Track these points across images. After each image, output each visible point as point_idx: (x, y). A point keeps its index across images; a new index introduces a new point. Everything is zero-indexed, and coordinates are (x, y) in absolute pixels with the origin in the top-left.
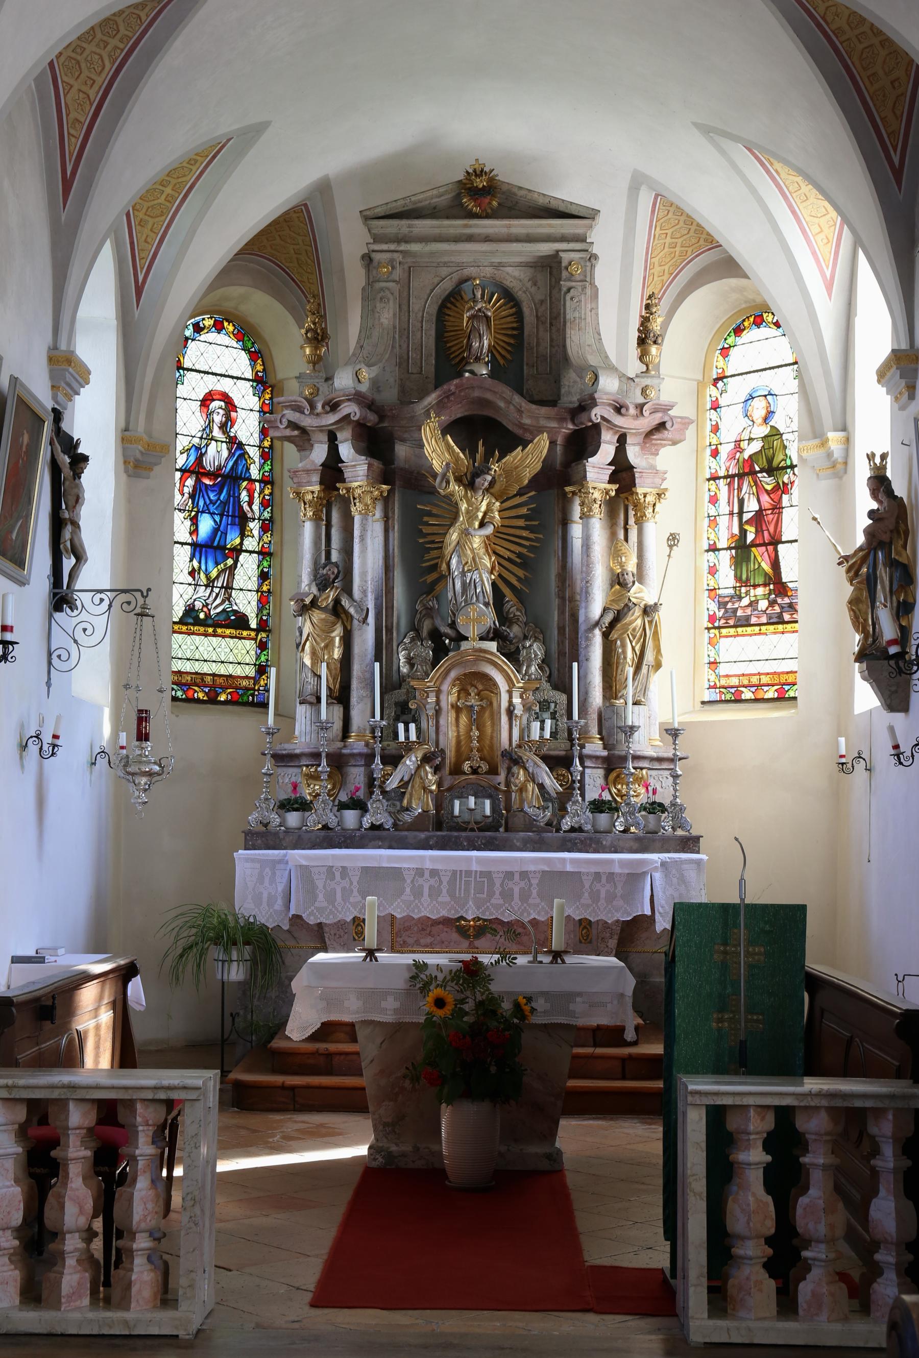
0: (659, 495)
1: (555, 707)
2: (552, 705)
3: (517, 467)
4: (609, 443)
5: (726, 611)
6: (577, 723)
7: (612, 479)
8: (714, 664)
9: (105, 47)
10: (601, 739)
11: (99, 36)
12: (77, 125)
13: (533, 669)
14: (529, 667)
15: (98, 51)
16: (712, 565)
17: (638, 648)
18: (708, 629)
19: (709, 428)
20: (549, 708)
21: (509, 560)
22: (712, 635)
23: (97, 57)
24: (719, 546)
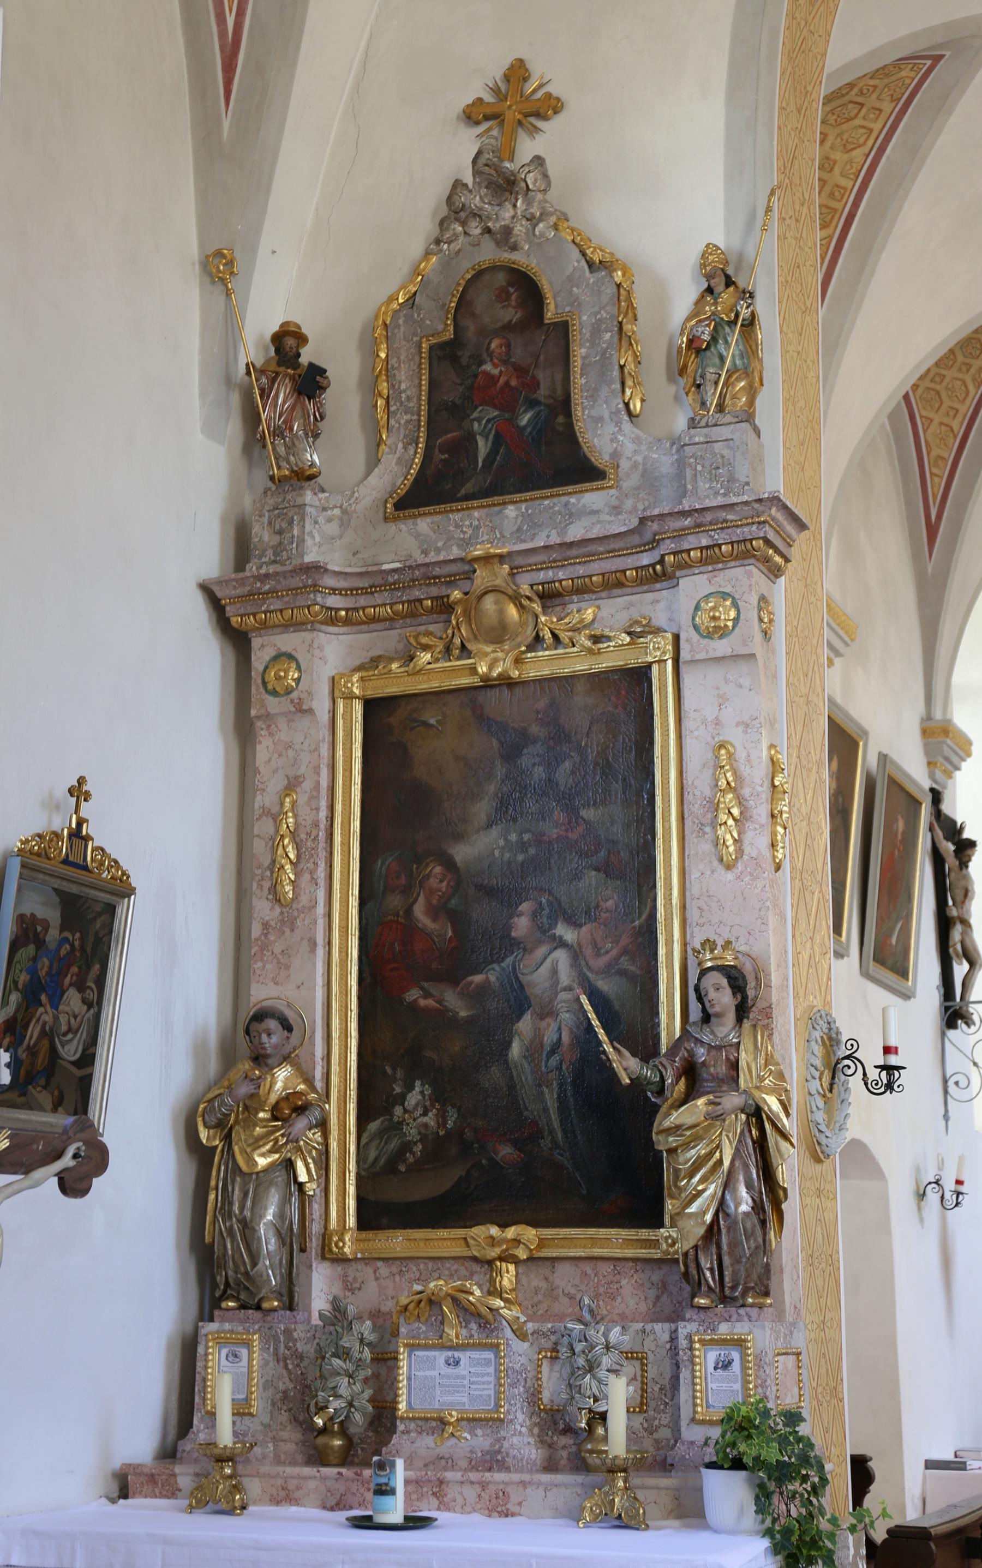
9: (968, 370)
11: (960, 358)
12: (940, 463)
15: (960, 376)
23: (959, 383)
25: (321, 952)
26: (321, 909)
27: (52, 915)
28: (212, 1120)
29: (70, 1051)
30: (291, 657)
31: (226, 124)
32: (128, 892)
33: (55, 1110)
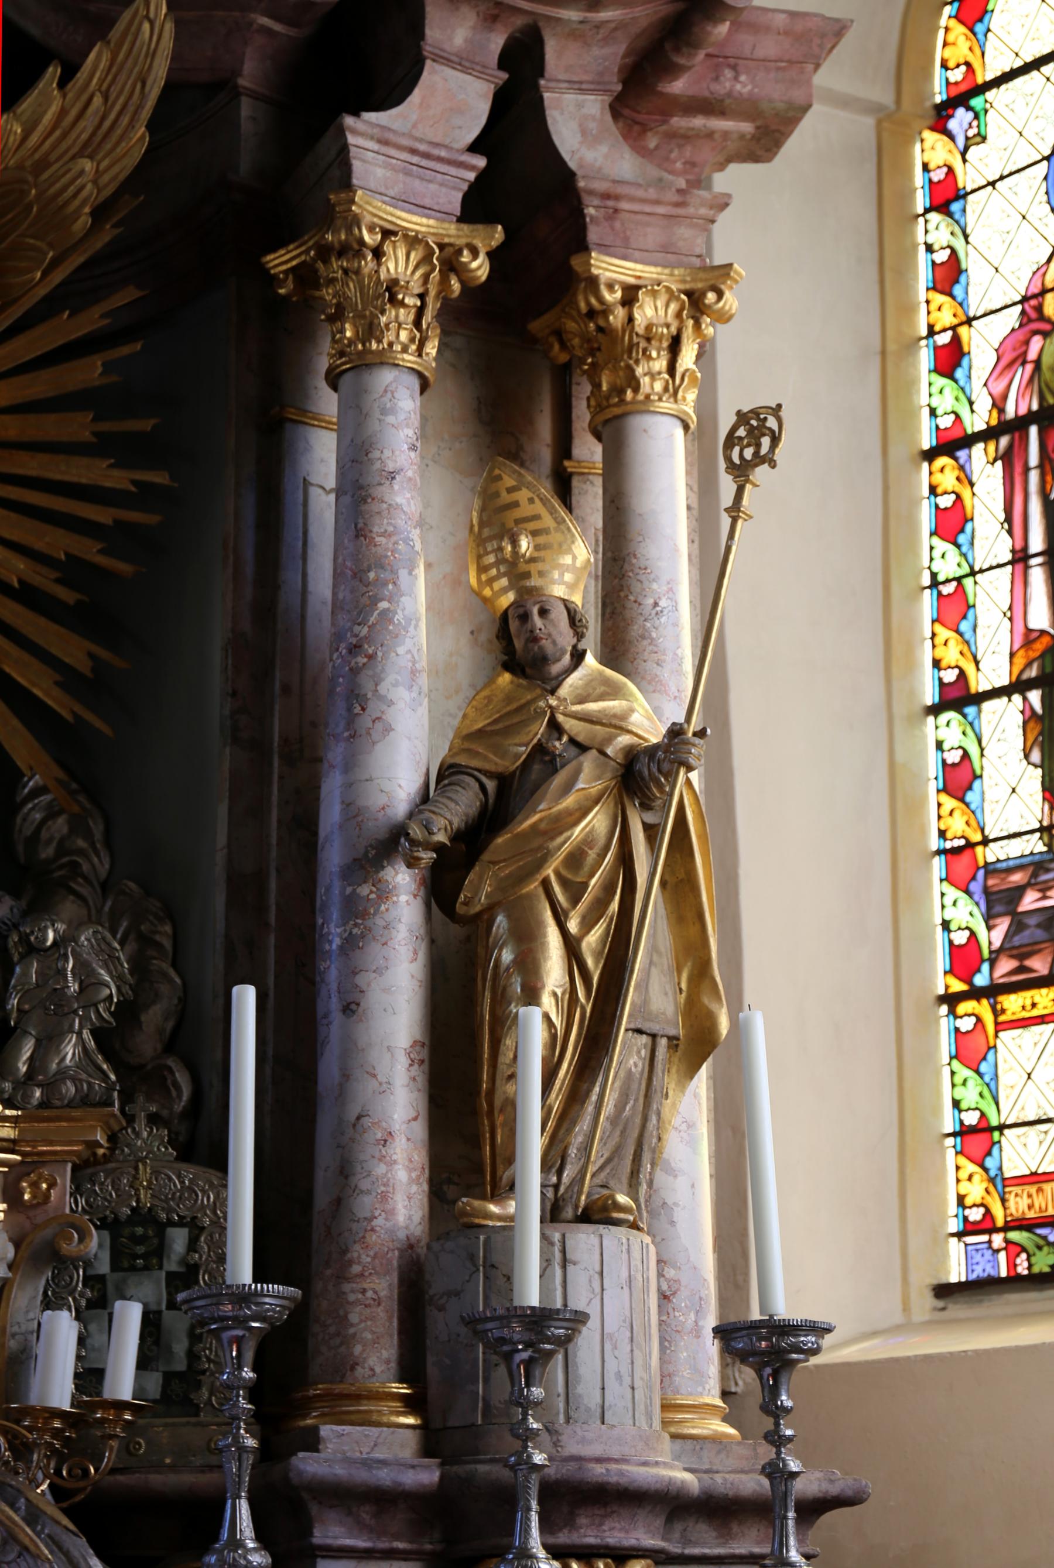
0: (695, 304)
1: (192, 1245)
2: (178, 1239)
3: (42, 165)
4: (462, 63)
5: (1018, 924)
6: (243, 1297)
7: (475, 207)
8: (978, 1137)
10: (411, 1404)
13: (70, 1051)
14: (48, 1042)
16: (954, 757)
17: (592, 940)
18: (951, 1000)
19: (924, 275)
20: (160, 1251)
21: (26, 595)
22: (966, 1024)
24: (979, 683)
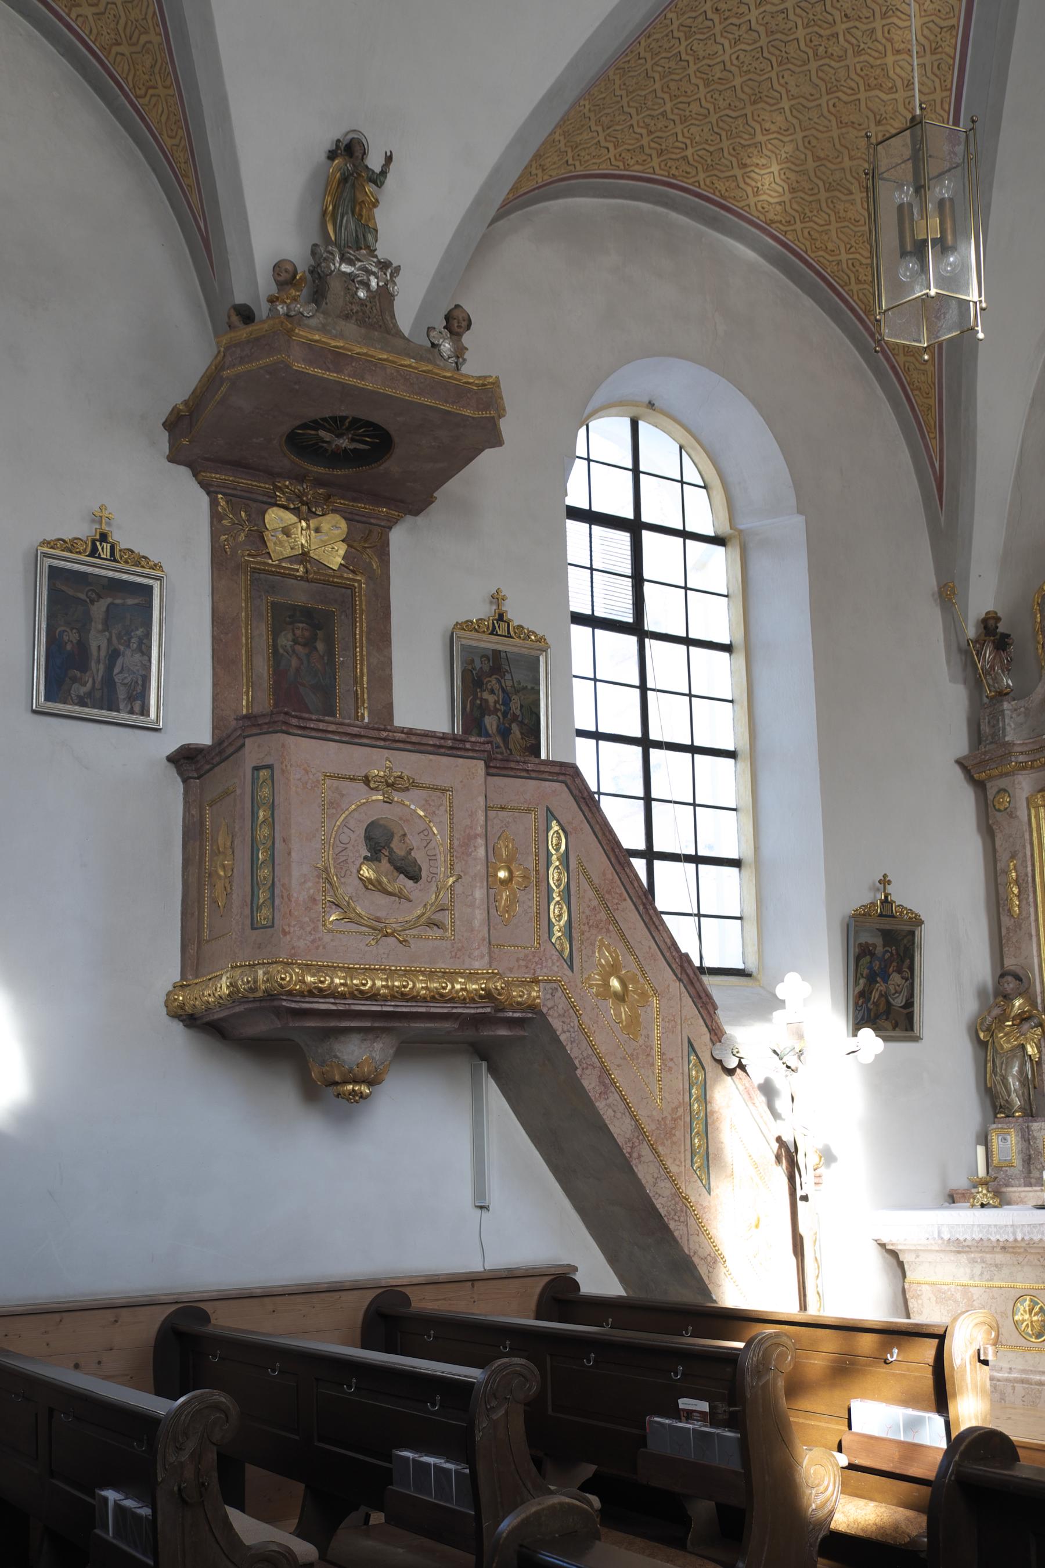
25: (1034, 939)
26: (1032, 918)
27: (879, 941)
28: (984, 1028)
29: (898, 1001)
30: (1005, 791)
31: (942, 519)
32: (921, 922)
33: (894, 1029)
